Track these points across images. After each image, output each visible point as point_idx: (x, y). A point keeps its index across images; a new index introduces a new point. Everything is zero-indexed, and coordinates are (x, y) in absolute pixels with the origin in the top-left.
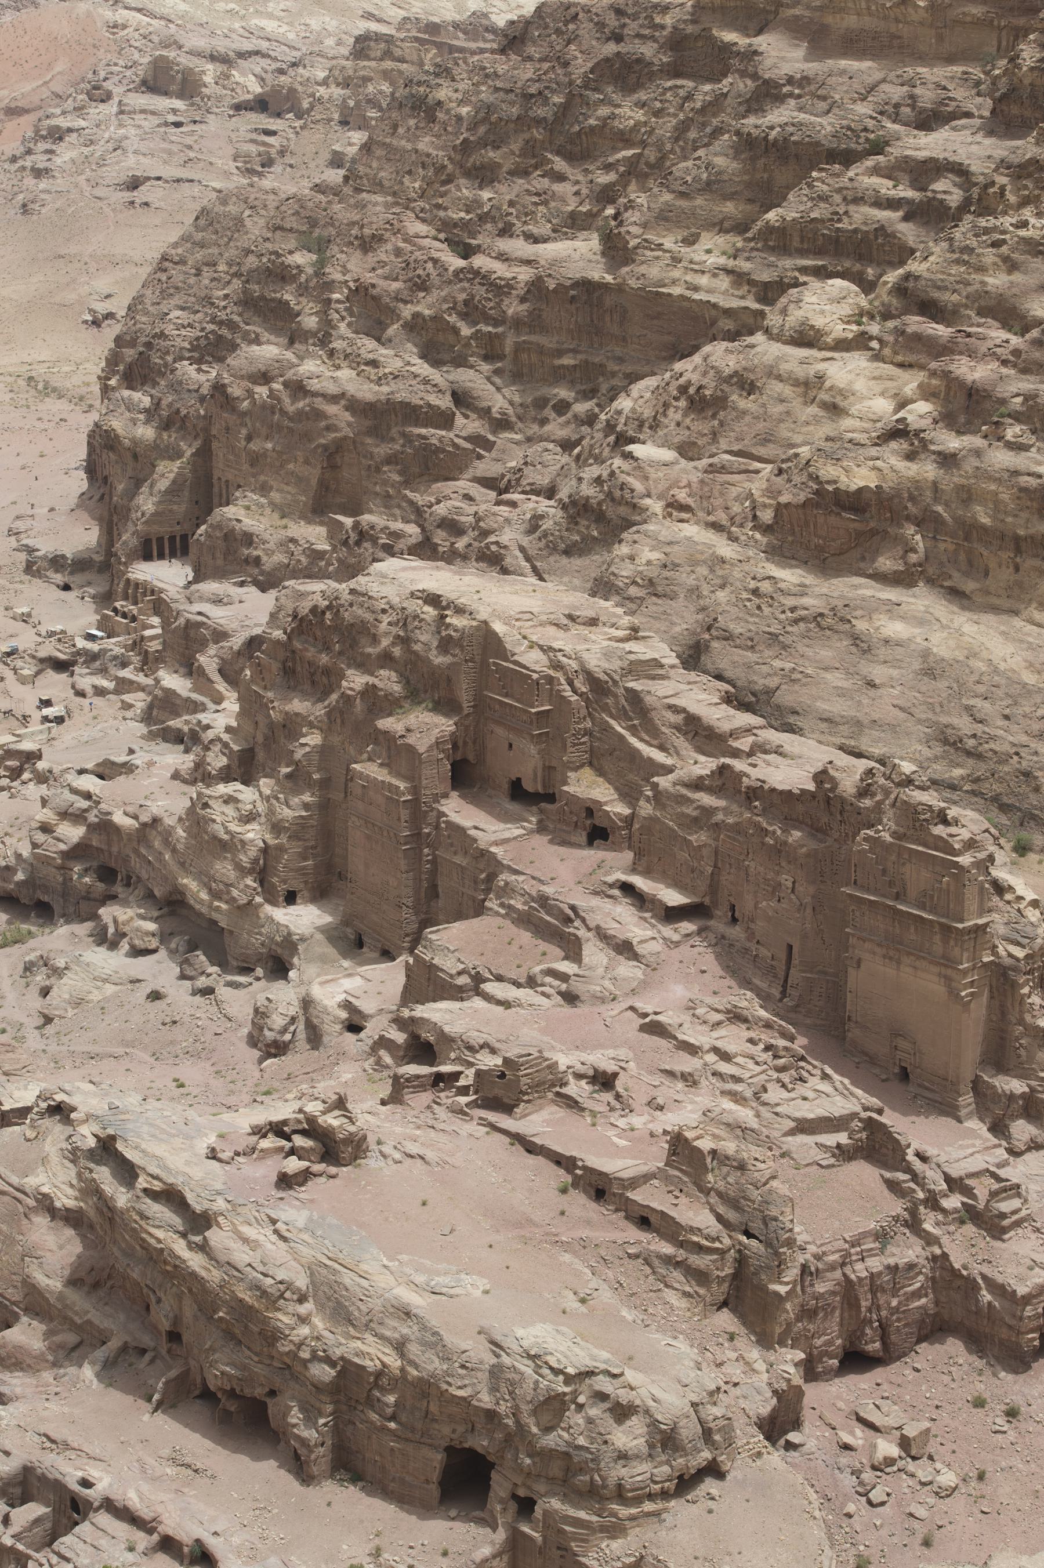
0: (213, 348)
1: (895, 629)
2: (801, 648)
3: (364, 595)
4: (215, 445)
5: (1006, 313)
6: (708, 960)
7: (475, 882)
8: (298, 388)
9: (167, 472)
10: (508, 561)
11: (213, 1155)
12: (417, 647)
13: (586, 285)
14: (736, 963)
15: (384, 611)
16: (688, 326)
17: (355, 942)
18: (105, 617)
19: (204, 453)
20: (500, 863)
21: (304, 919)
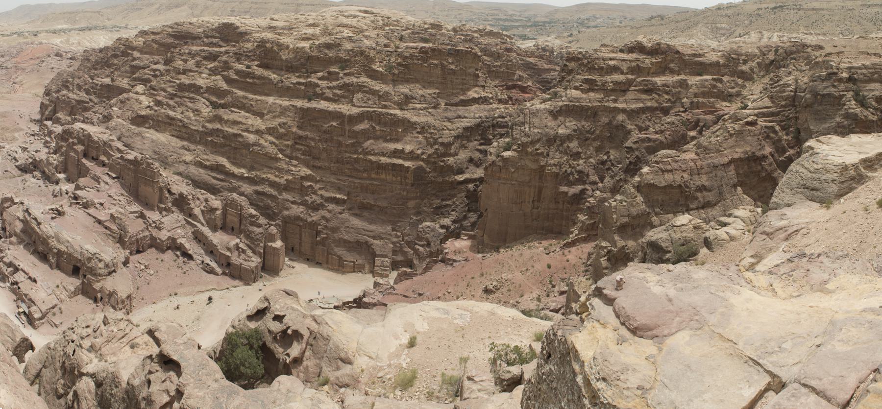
0: (58, 91)
1: (148, 135)
5: (164, 90)
6: (119, 185)
8: (68, 98)
9: (50, 108)
13: (108, 85)
14: (123, 186)
16: (123, 91)
17: (69, 180)
21: (62, 176)
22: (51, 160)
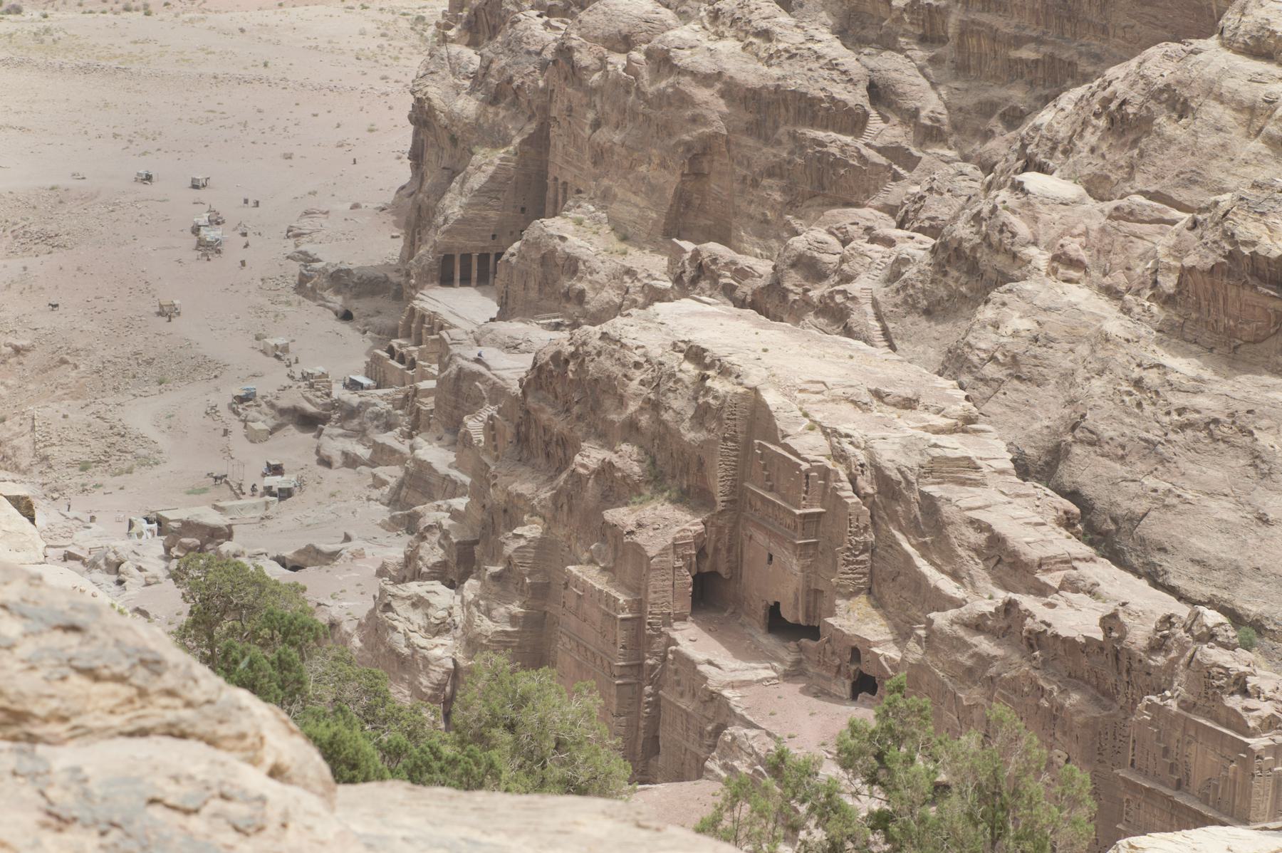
2: (1184, 464)
3: (617, 341)
4: (554, 131)
7: (701, 735)
8: (662, 61)
10: (855, 318)
12: (667, 416)
15: (637, 365)
18: (376, 359)
19: (539, 142)
20: (732, 711)
22: (407, 626)
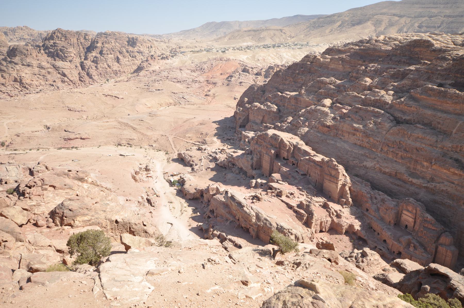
11: (245, 198)
